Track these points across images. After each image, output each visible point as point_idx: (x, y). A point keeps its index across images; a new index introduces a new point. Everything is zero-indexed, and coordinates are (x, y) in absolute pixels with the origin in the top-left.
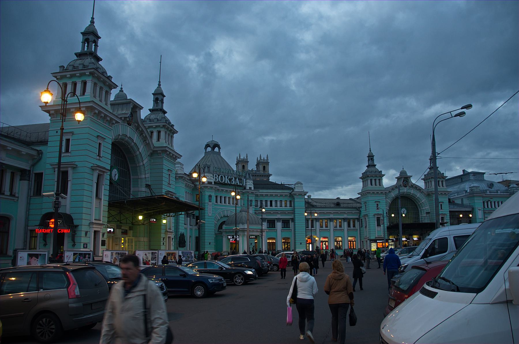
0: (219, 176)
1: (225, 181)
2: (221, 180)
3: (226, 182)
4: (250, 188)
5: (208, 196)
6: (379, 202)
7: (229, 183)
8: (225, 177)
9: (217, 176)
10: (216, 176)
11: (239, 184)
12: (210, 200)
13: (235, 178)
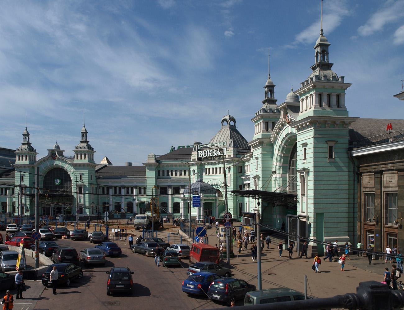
3: (209, 156)
4: (229, 156)
7: (211, 155)
8: (207, 151)
10: (200, 152)
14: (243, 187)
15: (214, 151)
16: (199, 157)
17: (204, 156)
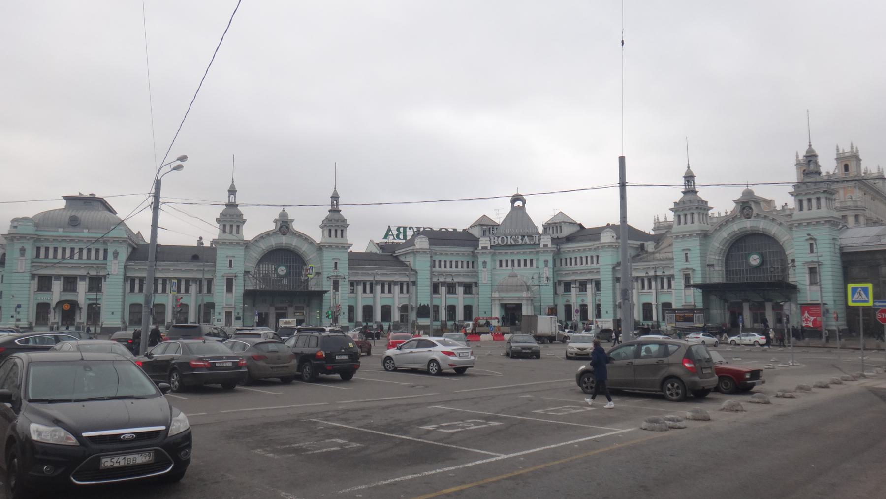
0: (498, 237)
1: (507, 240)
2: (501, 242)
3: (509, 243)
4: (545, 246)
5: (482, 262)
6: (689, 250)
8: (507, 238)
9: (496, 238)
11: (528, 243)
12: (485, 267)
13: (523, 237)
14: (559, 285)
15: (518, 237)
16: (492, 244)
17: (500, 243)
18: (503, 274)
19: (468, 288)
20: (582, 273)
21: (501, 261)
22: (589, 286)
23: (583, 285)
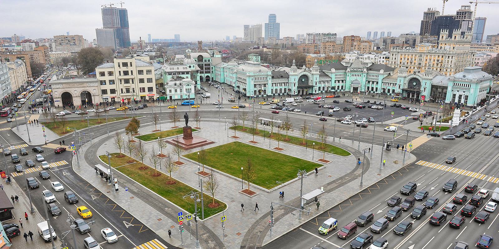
18: (354, 78)
19: (343, 81)
20: (374, 79)
21: (352, 75)
22: (375, 83)
23: (373, 82)
